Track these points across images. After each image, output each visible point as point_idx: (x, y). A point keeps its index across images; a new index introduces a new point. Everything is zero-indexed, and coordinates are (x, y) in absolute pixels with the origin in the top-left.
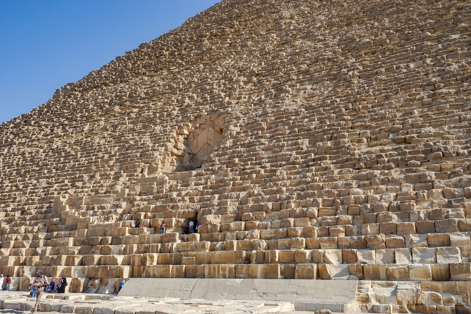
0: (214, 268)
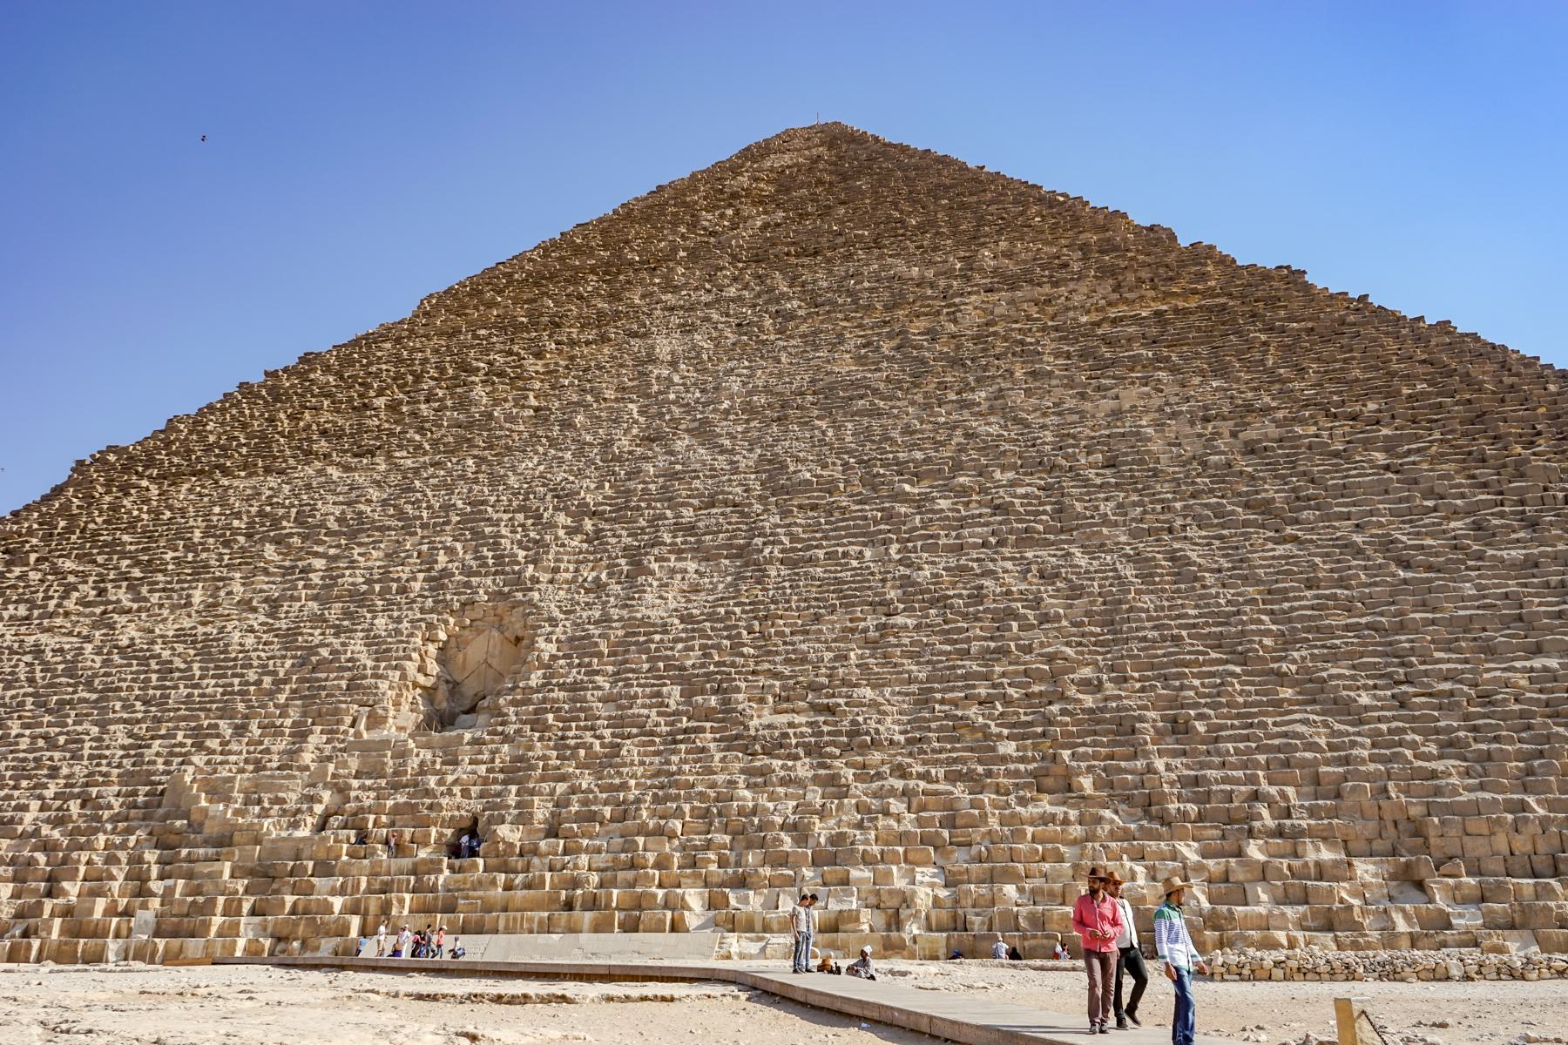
0: (515, 919)
